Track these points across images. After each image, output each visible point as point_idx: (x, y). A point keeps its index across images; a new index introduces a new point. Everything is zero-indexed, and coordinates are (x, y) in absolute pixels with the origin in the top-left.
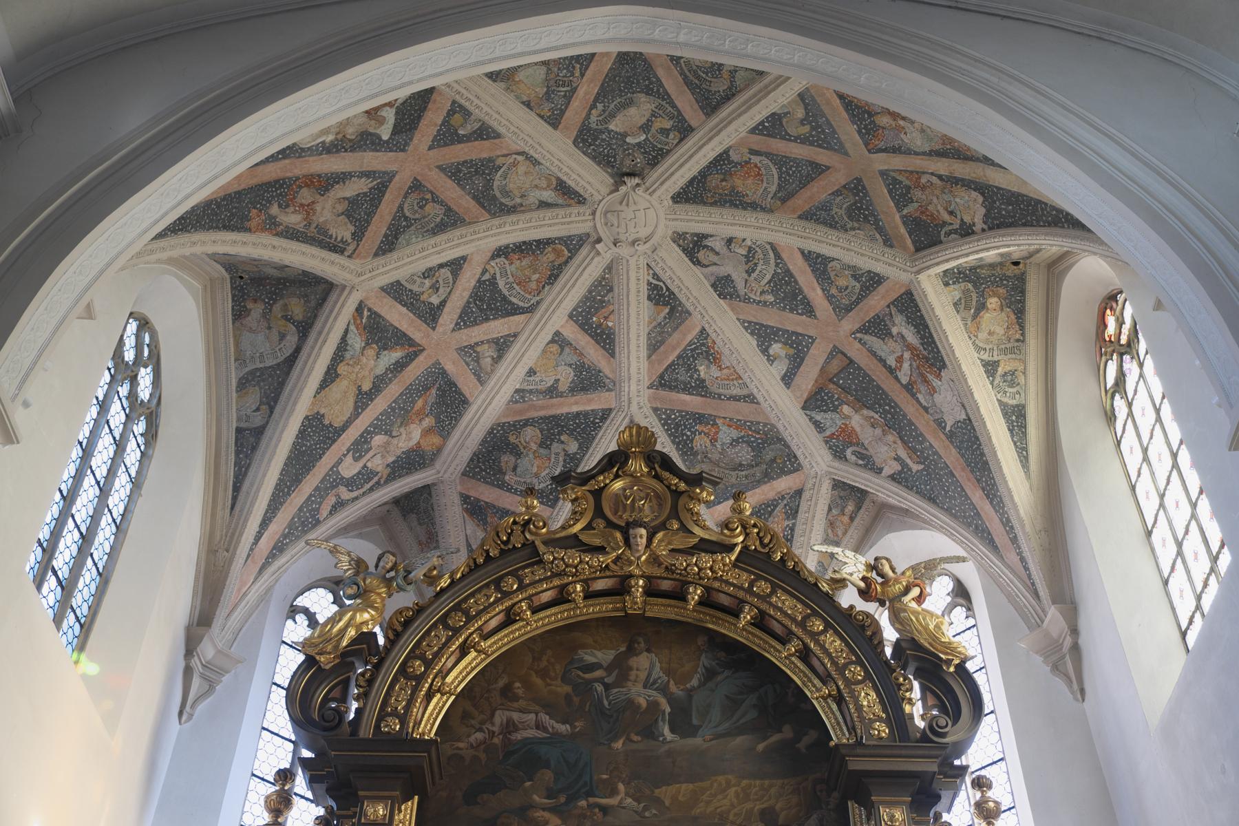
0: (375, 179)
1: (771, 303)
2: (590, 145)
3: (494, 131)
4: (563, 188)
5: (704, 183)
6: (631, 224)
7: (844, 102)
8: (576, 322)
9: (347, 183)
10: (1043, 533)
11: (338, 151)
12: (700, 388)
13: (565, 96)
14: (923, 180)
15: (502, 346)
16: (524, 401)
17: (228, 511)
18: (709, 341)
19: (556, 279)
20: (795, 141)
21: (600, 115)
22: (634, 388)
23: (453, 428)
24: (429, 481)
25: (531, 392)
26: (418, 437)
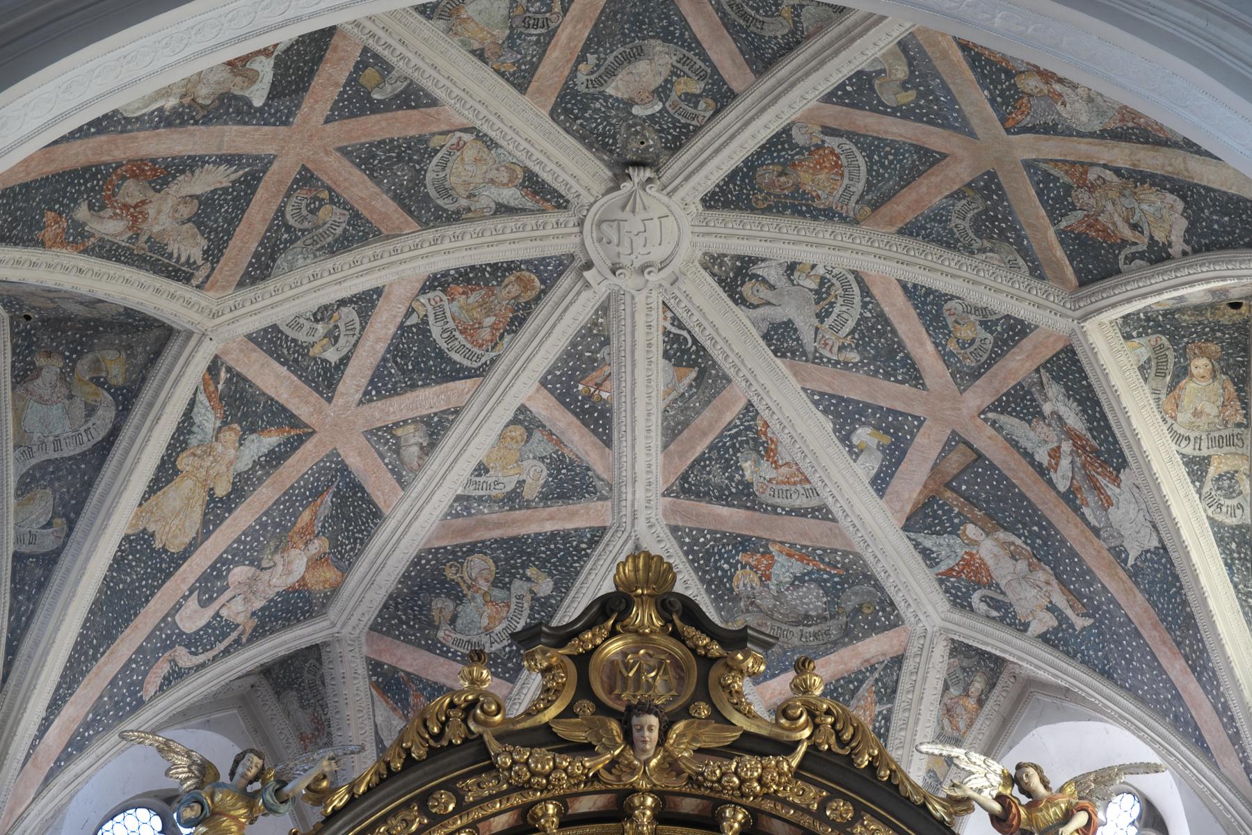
0: (240, 166)
1: (855, 364)
2: (577, 118)
3: (427, 95)
4: (534, 185)
5: (752, 179)
6: (639, 241)
7: (969, 55)
8: (552, 391)
9: (197, 172)
11: (183, 123)
12: (744, 496)
13: (538, 42)
14: (1092, 176)
16: (469, 514)
18: (760, 422)
19: (521, 324)
20: (893, 114)
21: (592, 73)
22: (640, 494)
23: (357, 556)
24: (318, 638)
25: (480, 499)
26: (303, 569)
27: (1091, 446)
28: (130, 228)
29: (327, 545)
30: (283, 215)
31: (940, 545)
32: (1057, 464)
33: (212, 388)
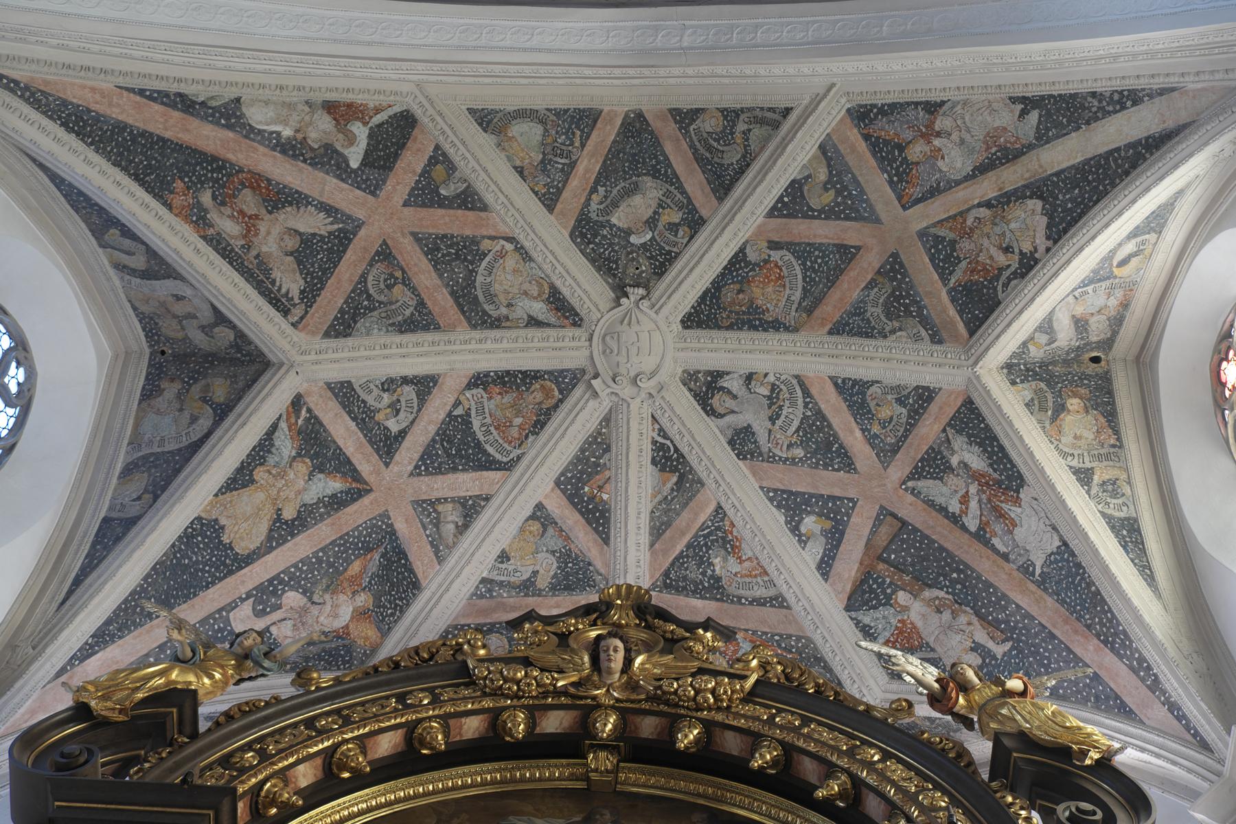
1: (801, 459)
2: (589, 243)
3: (480, 200)
5: (718, 298)
6: (634, 351)
8: (564, 492)
9: (302, 209)
10: (1195, 656)
11: (295, 157)
12: (714, 589)
13: (562, 170)
15: (470, 509)
16: (492, 597)
17: (55, 605)
18: (727, 523)
19: (542, 428)
20: (818, 217)
21: (601, 203)
25: (501, 584)
26: (348, 617)
27: (993, 480)
28: (245, 237)
29: (371, 601)
30: (365, 282)
31: (877, 619)
32: (967, 508)
33: (293, 420)
